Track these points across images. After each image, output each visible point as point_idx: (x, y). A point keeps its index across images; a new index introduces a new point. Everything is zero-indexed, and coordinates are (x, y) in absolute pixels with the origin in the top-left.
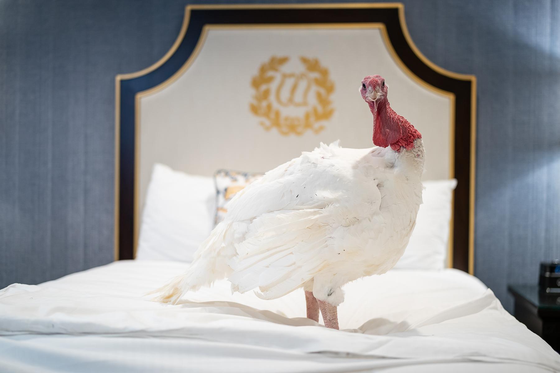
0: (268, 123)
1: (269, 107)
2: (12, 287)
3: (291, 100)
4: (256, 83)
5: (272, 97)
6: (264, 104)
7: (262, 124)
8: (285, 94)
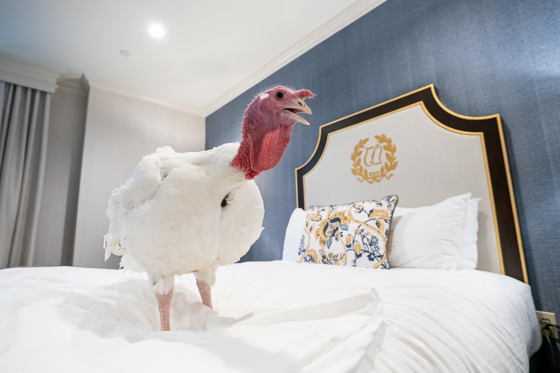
0: (361, 178)
1: (361, 168)
3: (372, 162)
5: (362, 163)
6: (358, 167)
7: (358, 179)
8: (369, 160)
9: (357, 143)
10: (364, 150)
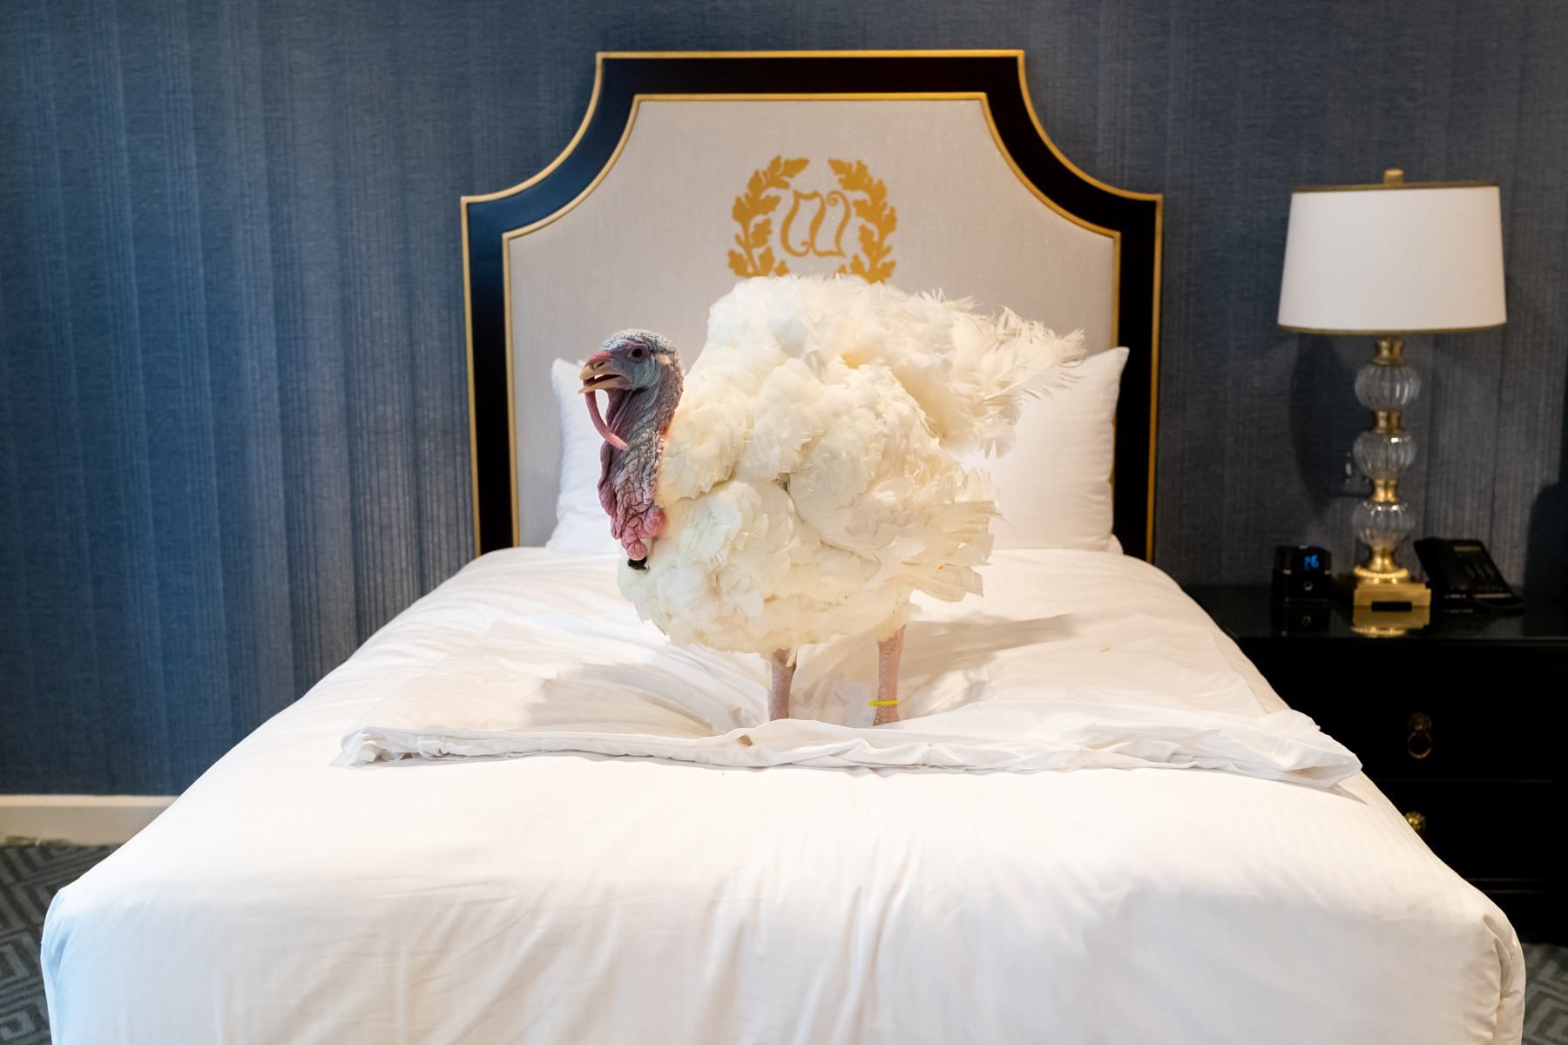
2: (56, 962)
3: (810, 244)
4: (742, 212)
5: (774, 240)
6: (757, 252)
8: (799, 233)
9: (763, 165)
10: (787, 199)
